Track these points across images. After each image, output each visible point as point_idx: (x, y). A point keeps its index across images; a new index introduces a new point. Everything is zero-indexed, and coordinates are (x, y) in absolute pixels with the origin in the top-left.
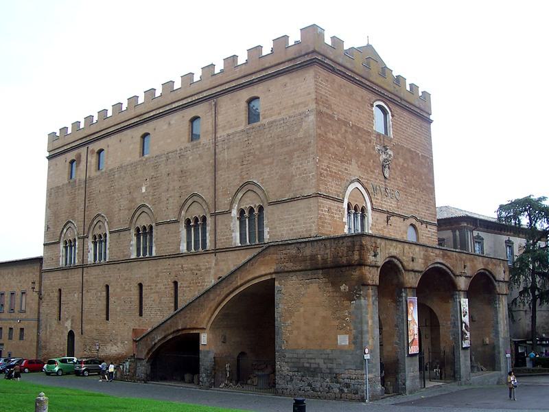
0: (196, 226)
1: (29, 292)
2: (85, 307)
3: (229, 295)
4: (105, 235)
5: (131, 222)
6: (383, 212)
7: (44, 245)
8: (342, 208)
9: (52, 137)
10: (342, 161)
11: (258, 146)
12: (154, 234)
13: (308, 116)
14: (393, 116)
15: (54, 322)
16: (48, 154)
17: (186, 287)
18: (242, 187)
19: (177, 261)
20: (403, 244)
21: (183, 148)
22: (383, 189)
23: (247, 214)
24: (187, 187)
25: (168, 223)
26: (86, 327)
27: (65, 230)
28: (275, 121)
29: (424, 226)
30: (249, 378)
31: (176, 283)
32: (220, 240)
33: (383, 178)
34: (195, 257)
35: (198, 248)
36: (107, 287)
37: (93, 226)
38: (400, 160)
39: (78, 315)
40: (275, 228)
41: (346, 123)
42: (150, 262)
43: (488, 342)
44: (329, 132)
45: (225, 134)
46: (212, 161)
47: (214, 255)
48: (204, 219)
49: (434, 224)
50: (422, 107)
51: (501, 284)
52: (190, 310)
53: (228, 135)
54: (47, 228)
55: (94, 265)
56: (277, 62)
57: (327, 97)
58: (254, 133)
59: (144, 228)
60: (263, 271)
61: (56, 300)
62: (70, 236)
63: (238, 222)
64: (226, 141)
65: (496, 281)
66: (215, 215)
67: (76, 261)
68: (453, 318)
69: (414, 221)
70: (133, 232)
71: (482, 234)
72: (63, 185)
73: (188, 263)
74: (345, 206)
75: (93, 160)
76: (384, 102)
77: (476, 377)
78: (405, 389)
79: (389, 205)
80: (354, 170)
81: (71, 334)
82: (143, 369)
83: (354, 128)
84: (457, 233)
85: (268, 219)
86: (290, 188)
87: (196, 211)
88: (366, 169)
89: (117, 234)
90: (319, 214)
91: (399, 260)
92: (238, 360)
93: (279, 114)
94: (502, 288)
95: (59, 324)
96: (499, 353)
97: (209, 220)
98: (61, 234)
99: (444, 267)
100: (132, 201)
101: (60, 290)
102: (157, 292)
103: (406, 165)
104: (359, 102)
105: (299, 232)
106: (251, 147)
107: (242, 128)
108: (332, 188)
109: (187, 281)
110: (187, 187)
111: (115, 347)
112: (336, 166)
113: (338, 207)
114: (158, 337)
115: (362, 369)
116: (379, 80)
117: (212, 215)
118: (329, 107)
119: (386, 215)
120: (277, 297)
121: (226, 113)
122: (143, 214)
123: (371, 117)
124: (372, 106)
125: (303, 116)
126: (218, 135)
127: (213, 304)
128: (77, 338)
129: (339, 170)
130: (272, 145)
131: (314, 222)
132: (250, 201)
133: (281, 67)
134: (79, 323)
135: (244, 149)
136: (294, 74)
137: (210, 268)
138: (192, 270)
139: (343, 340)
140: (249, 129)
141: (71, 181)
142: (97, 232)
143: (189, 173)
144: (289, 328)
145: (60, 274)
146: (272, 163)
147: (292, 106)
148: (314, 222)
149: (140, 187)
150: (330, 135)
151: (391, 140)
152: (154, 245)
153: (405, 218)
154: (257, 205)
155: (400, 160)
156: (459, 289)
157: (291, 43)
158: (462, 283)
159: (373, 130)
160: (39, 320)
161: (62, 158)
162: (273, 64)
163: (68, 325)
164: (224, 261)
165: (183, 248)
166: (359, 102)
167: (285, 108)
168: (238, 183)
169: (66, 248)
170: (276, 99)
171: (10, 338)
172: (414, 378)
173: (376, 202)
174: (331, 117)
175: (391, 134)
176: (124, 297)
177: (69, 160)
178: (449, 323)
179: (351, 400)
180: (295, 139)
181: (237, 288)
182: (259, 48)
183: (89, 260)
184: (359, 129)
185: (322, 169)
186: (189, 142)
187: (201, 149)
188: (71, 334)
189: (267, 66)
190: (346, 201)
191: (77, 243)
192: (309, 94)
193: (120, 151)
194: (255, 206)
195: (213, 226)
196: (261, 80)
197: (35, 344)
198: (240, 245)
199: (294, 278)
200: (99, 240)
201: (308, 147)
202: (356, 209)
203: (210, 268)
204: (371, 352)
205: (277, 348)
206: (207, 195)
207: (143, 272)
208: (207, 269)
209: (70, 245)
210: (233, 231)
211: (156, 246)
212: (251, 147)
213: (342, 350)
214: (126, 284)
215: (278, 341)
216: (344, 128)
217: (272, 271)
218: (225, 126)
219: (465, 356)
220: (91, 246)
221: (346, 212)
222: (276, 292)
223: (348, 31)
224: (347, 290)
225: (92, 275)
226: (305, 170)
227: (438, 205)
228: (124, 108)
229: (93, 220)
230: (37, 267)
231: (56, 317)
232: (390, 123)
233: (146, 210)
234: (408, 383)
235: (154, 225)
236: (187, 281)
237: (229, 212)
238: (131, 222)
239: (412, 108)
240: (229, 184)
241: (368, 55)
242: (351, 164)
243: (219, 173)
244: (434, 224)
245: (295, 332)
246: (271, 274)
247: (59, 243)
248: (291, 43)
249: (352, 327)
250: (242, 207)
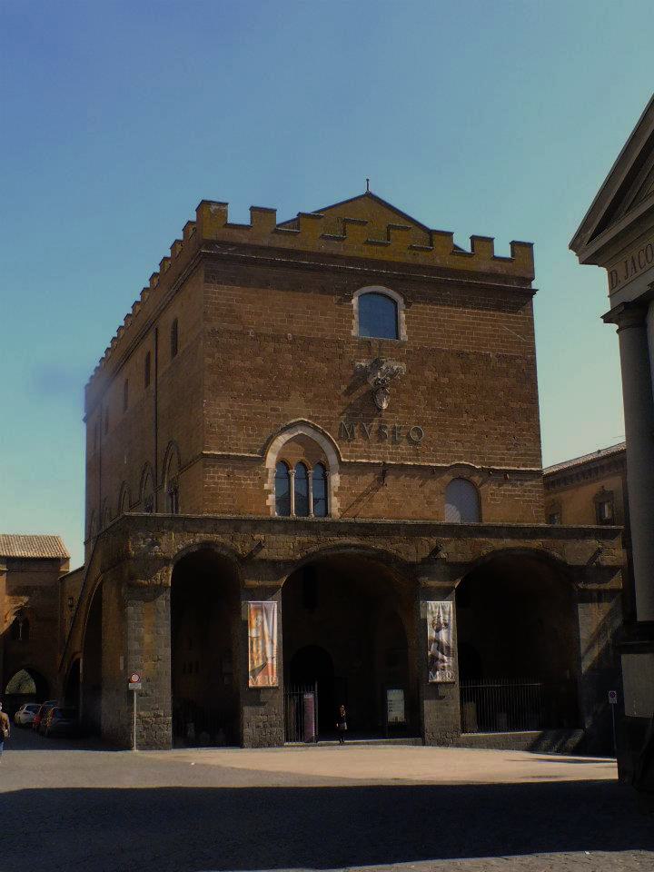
38: (427, 373)
41: (276, 339)
57: (230, 305)
155: (427, 373)
185: (215, 416)
216: (270, 347)
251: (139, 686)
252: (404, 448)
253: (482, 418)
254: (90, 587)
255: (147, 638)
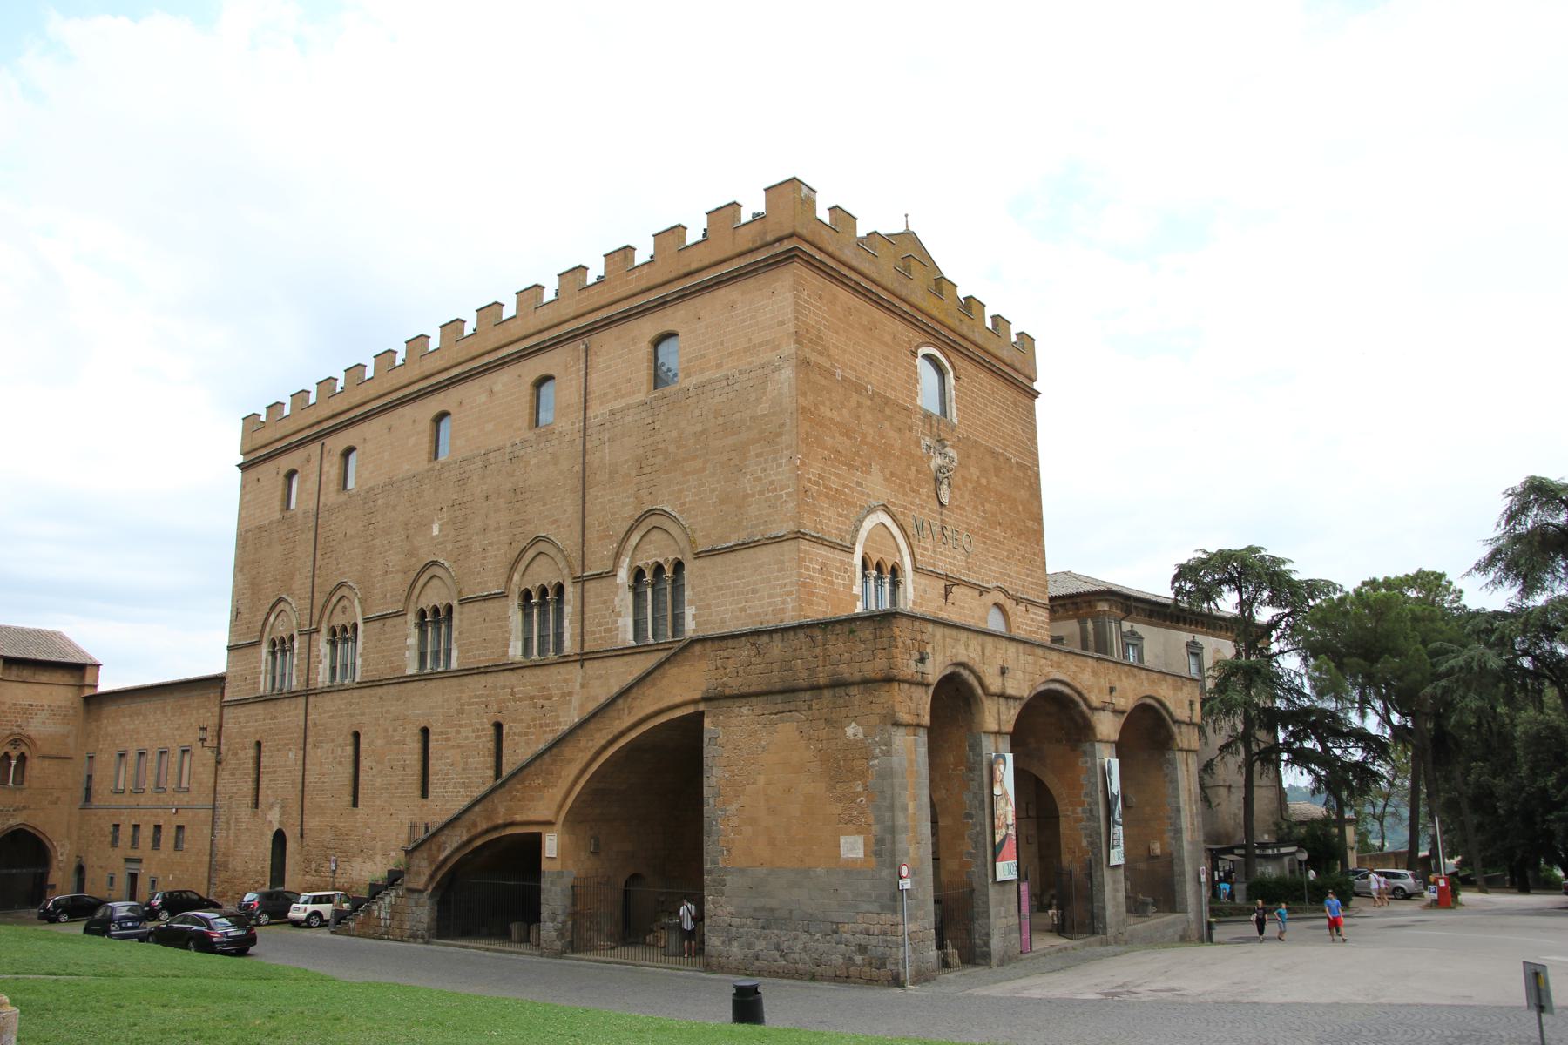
0: (543, 604)
1: (197, 748)
2: (310, 778)
3: (605, 748)
4: (355, 627)
5: (408, 598)
6: (938, 576)
7: (230, 648)
8: (851, 565)
9: (251, 421)
10: (850, 467)
11: (674, 434)
12: (455, 621)
13: (777, 369)
14: (957, 378)
15: (245, 812)
16: (241, 460)
17: (520, 735)
18: (639, 521)
19: (503, 679)
20: (980, 638)
21: (518, 440)
22: (937, 529)
23: (648, 578)
24: (528, 522)
25: (485, 598)
26: (312, 823)
27: (272, 618)
28: (710, 382)
29: (1022, 607)
30: (652, 931)
31: (498, 727)
32: (593, 633)
33: (937, 507)
34: (538, 671)
35: (547, 651)
36: (356, 735)
37: (330, 607)
38: (973, 470)
39: (294, 795)
40: (708, 606)
41: (859, 388)
42: (446, 682)
43: (1158, 851)
44: (823, 403)
45: (605, 409)
46: (578, 468)
47: (578, 665)
48: (560, 589)
49: (1042, 606)
50: (1018, 365)
51: (1184, 728)
52: (522, 782)
53: (612, 413)
54: (237, 614)
55: (331, 690)
56: (714, 259)
58: (665, 408)
59: (436, 610)
60: (681, 688)
61: (250, 765)
62: (281, 628)
63: (630, 596)
64: (608, 425)
65: (1175, 722)
66: (581, 580)
67: (294, 683)
68: (1087, 800)
69: (1001, 598)
70: (411, 618)
71: (1140, 629)
72: (271, 523)
73: (526, 683)
74: (857, 561)
75: (332, 469)
76: (943, 352)
77: (1139, 926)
78: (989, 954)
79: (949, 561)
80: (876, 485)
81: (279, 839)
82: (422, 913)
83: (877, 400)
84: (1090, 625)
85: (693, 588)
86: (740, 522)
87: (543, 574)
88: (901, 486)
89: (378, 624)
90: (800, 575)
91: (972, 671)
92: (626, 893)
93: (719, 366)
94: (1186, 738)
95: (255, 815)
96: (1183, 874)
97: (570, 592)
98: (264, 624)
99: (1067, 690)
100: (411, 553)
101: (259, 744)
102: (459, 746)
103: (984, 481)
104: (886, 344)
105: (758, 615)
106: (658, 438)
107: (640, 397)
108: (830, 522)
109: (521, 721)
110: (528, 522)
111: (369, 865)
112: (838, 476)
113: (842, 562)
114: (453, 841)
115: (895, 912)
116: (930, 304)
117: (576, 581)
118: (824, 352)
119: (942, 583)
120: (708, 751)
121: (609, 367)
122: (435, 582)
123: (913, 378)
124: (915, 354)
125: (768, 370)
126: (590, 414)
127: (574, 770)
128: (291, 845)
129: (845, 486)
130: (703, 432)
131: (789, 593)
132: (656, 551)
133: (724, 269)
134: (296, 814)
135: (645, 442)
136: (750, 283)
137: (570, 694)
138: (532, 698)
139: (853, 848)
140: (656, 399)
141: (288, 514)
142: (339, 620)
143: (528, 495)
144: (735, 821)
145: (259, 709)
146: (704, 469)
147: (746, 350)
148: (789, 593)
149: (429, 526)
150: (825, 411)
151: (953, 428)
152: (454, 646)
153: (982, 591)
154: (671, 558)
155: (973, 470)
156: (1099, 737)
157: (746, 216)
158: (1107, 727)
159: (916, 406)
160: (214, 808)
161: (270, 466)
162: (707, 263)
163: (274, 818)
164: (600, 677)
165: (515, 651)
166: (886, 344)
167: (730, 354)
168: (630, 512)
169: (273, 654)
170: (710, 335)
171: (156, 843)
172: (1007, 931)
173: (923, 555)
174: (828, 373)
175: (954, 415)
176: (389, 762)
177: (284, 471)
178: (1079, 810)
179: (872, 981)
180: (753, 418)
181: (623, 733)
182: (679, 229)
183: (320, 679)
184: (886, 401)
185: (809, 480)
186: (530, 428)
187: (555, 442)
188: (279, 839)
189: (694, 267)
190: (859, 552)
191: (296, 645)
192: (782, 323)
193: (386, 450)
194: (666, 560)
195: (579, 605)
196: (683, 296)
197: (207, 859)
198: (633, 643)
199: (745, 710)
200: (342, 636)
201: (778, 435)
202: (879, 567)
203: (570, 694)
204: (913, 873)
205: (707, 866)
206: (566, 538)
207: (429, 704)
208: (563, 695)
209: (281, 647)
210: (619, 615)
211: (459, 646)
212: (658, 438)
213: (850, 870)
214: (395, 730)
215: (708, 847)
217: (698, 695)
218: (605, 395)
219: (1115, 882)
220: (324, 648)
221: (859, 574)
222: (706, 740)
223: (869, 195)
224: (861, 736)
225: (325, 710)
226: (772, 482)
227: (1050, 570)
228: (399, 362)
229: (331, 594)
230: (213, 694)
231: (249, 800)
232: (952, 393)
233: (439, 571)
234: (996, 943)
235: (455, 603)
236: (521, 721)
237: (612, 574)
238: (408, 598)
239: (1001, 366)
240: (613, 514)
241: (907, 250)
242: (869, 473)
243: (591, 493)
244: (1042, 606)
245: (748, 830)
246: (695, 702)
247: (258, 643)
248: (746, 216)
249: (871, 819)
250: (640, 564)
251: (908, 886)
252: (960, 560)
253: (1009, 534)
254: (627, 721)
255: (911, 806)
